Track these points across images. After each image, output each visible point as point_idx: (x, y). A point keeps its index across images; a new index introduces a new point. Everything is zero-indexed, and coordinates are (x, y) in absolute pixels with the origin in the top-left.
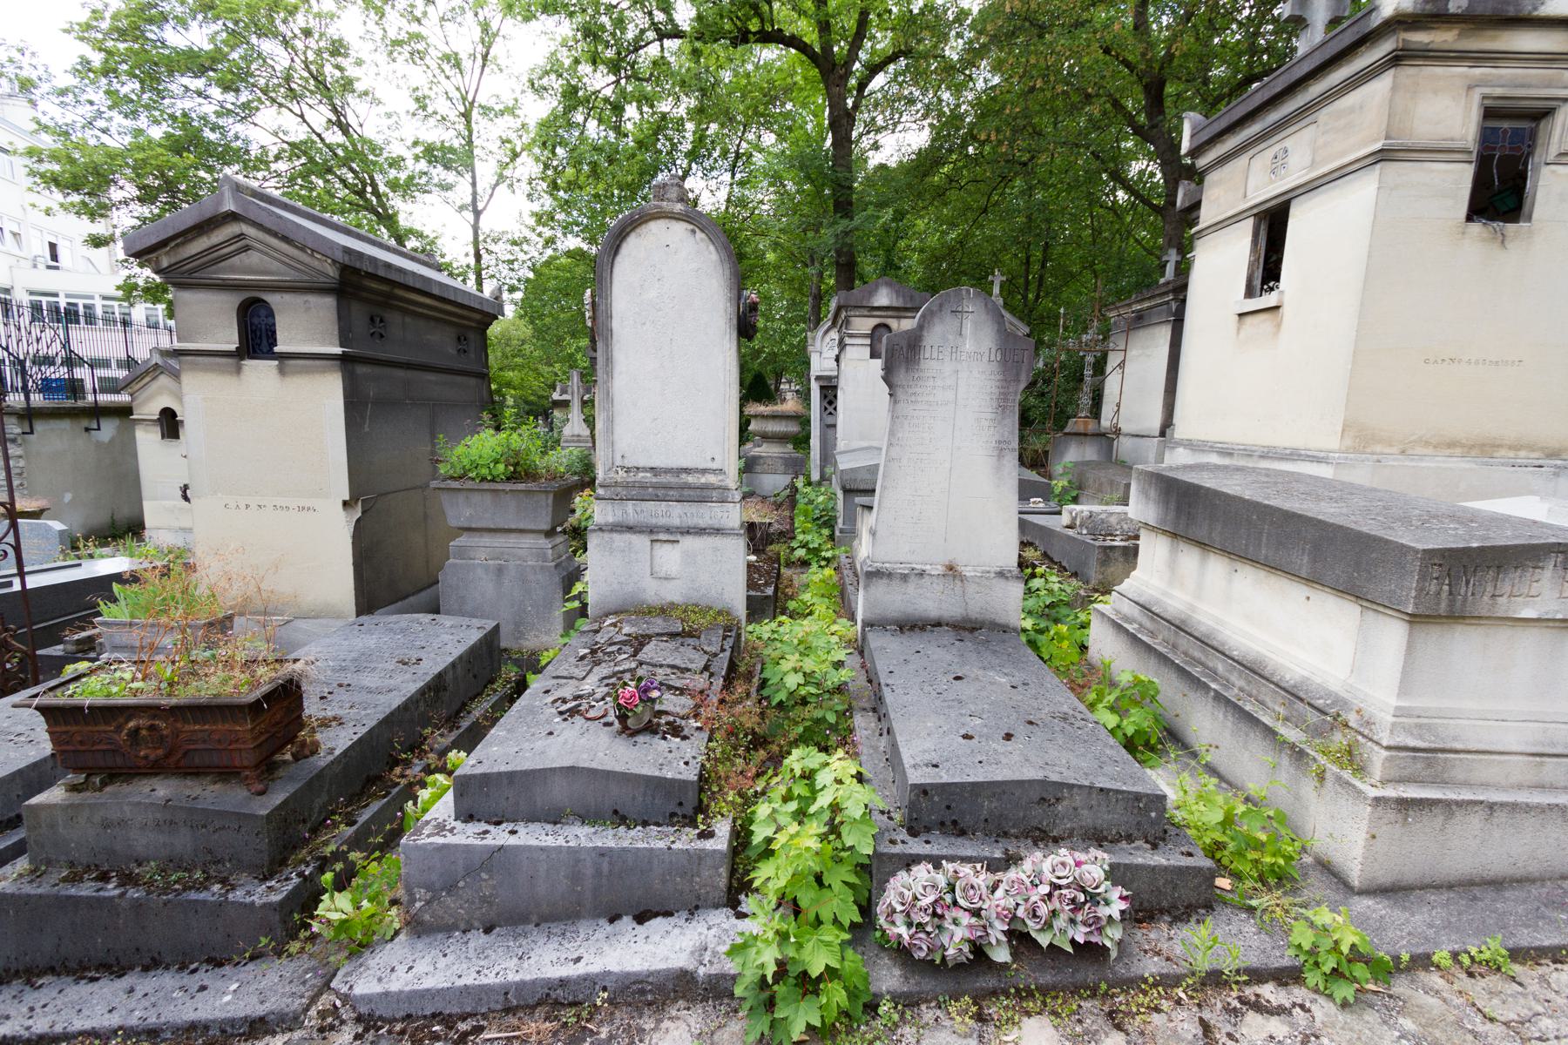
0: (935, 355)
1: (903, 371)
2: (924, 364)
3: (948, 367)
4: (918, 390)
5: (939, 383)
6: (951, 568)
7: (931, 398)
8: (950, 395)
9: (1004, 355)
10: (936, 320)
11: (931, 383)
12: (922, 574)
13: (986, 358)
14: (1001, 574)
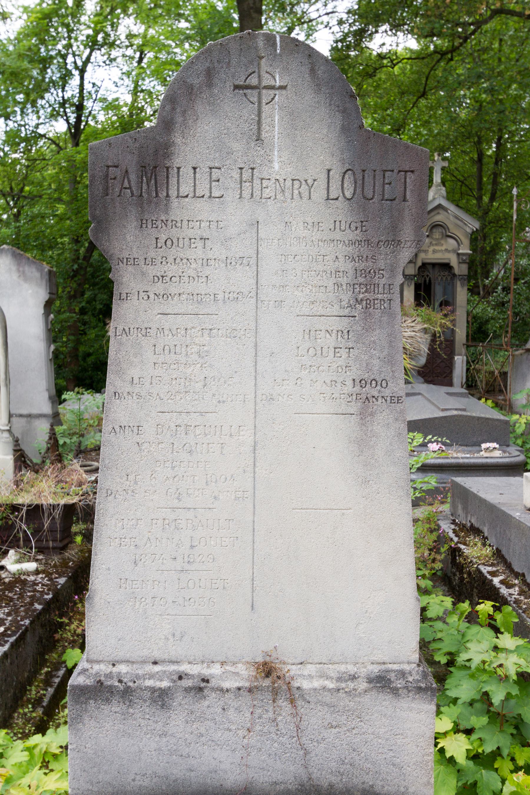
0: (203, 189)
1: (132, 225)
2: (179, 210)
3: (234, 214)
4: (171, 269)
5: (217, 251)
6: (267, 670)
7: (201, 287)
8: (243, 279)
9: (360, 184)
10: (200, 107)
11: (197, 252)
12: (201, 687)
13: (319, 193)
14: (382, 682)
